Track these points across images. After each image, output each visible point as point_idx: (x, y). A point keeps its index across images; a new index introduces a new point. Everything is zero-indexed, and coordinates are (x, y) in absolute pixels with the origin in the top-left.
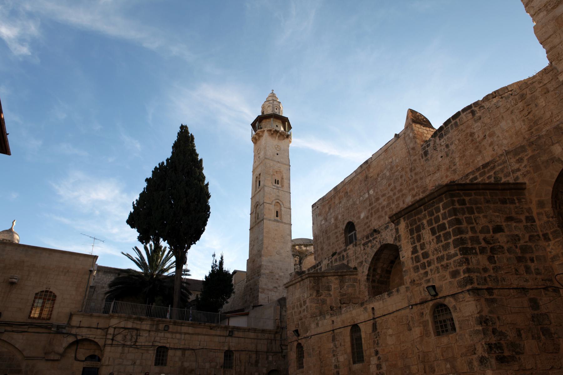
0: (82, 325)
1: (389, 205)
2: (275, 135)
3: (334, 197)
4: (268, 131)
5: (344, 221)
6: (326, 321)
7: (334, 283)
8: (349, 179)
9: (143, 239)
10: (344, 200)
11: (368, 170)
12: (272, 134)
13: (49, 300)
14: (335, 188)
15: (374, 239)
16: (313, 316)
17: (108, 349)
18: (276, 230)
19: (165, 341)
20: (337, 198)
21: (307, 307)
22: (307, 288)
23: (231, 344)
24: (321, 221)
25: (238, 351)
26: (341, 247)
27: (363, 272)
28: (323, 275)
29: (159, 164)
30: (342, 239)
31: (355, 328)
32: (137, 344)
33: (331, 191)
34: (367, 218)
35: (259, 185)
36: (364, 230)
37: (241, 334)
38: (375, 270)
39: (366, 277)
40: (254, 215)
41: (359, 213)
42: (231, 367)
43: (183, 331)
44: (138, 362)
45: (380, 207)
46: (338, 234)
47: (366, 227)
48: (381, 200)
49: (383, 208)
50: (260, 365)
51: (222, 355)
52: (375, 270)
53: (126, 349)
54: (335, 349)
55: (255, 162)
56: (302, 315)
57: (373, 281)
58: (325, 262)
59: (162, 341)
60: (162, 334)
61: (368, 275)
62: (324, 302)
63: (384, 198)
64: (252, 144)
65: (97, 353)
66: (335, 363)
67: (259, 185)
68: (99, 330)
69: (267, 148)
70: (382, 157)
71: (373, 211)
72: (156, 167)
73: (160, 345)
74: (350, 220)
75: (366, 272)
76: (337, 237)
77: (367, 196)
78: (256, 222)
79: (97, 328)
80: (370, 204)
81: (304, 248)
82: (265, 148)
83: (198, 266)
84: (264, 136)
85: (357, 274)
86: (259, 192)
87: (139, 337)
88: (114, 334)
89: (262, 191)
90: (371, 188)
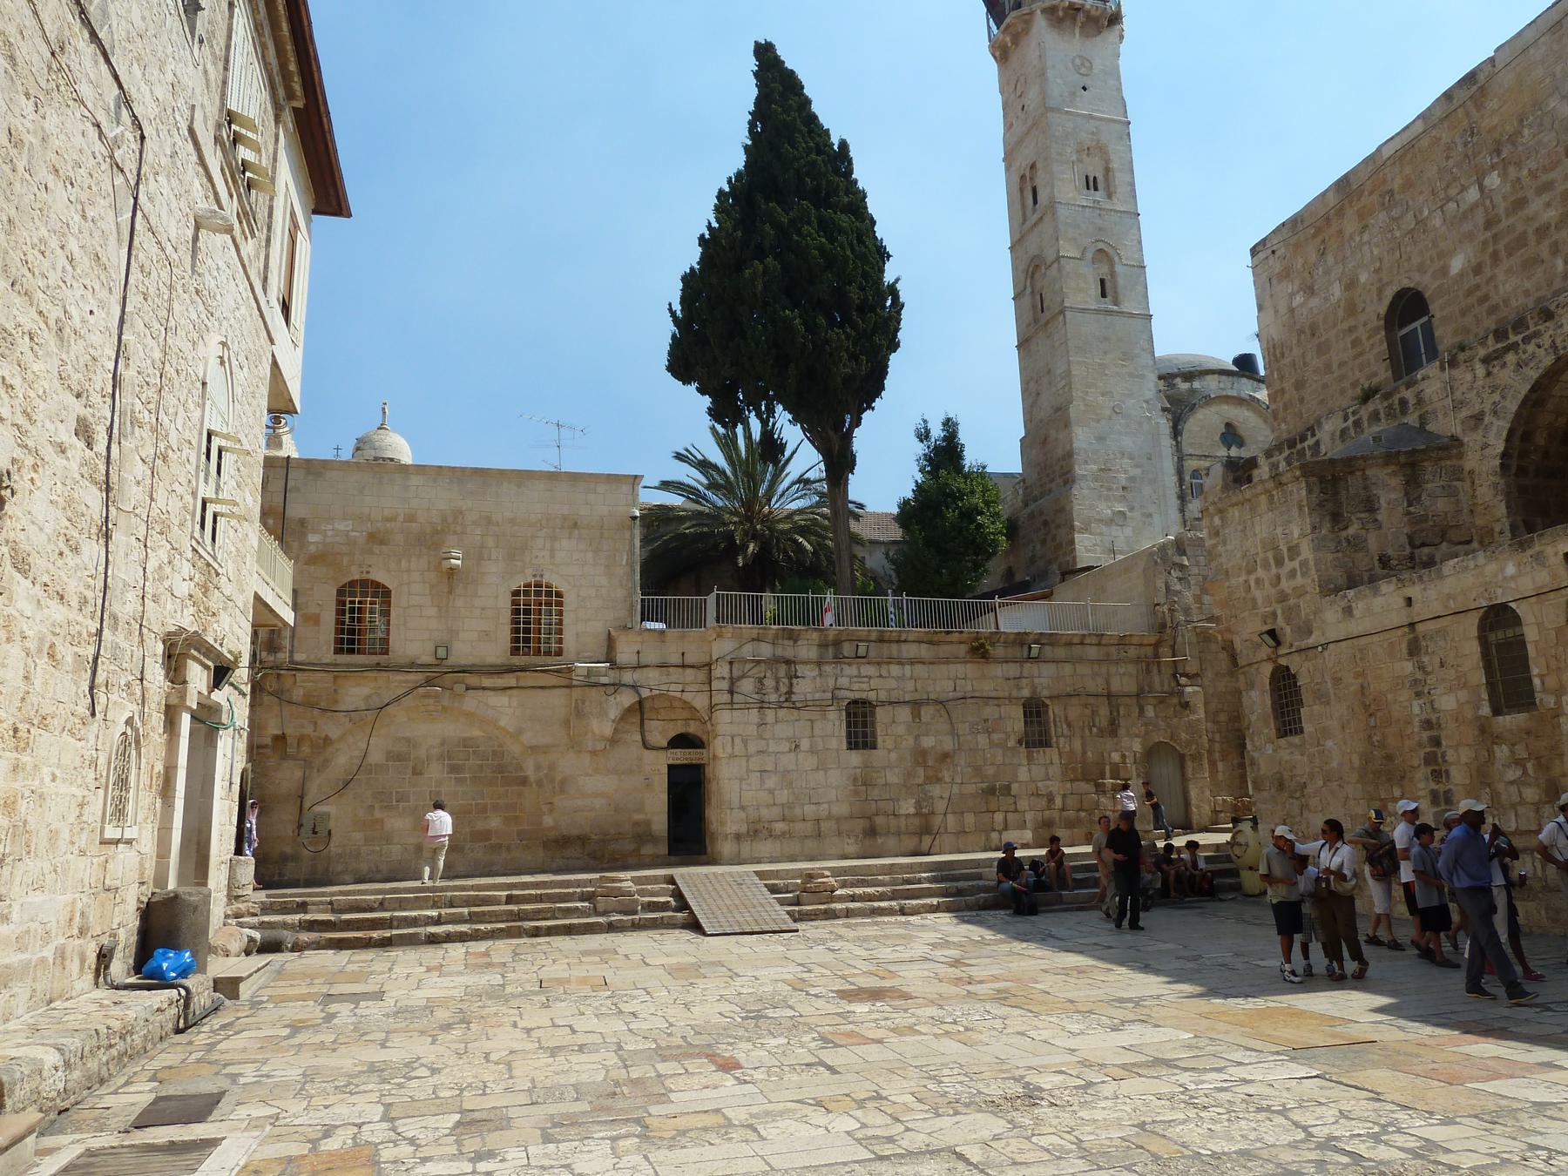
0: (644, 661)
2: (1068, 23)
3: (1340, 212)
4: (1044, 11)
5: (1380, 291)
6: (1378, 602)
7: (1388, 488)
8: (1397, 145)
9: (725, 413)
11: (1479, 106)
12: (1060, 21)
13: (549, 604)
14: (1343, 184)
15: (1526, 340)
16: (1329, 589)
17: (724, 718)
18: (1106, 339)
19: (865, 686)
20: (1350, 213)
21: (1304, 564)
22: (1301, 507)
23: (1036, 681)
24: (1292, 296)
25: (1058, 697)
26: (1376, 374)
27: (1485, 446)
28: (1349, 464)
29: (729, 181)
30: (1377, 347)
31: (1498, 618)
32: (794, 698)
33: (1324, 194)
34: (1478, 269)
35: (1035, 202)
36: (1463, 313)
37: (1061, 652)
38: (1527, 437)
39: (1498, 462)
40: (1027, 300)
42: (1045, 743)
43: (905, 655)
44: (805, 744)
45: (1530, 231)
46: (1362, 333)
47: (1473, 299)
48: (1536, 204)
49: (1542, 232)
50: (1122, 731)
51: (1018, 713)
52: (1527, 437)
53: (770, 715)
54: (1419, 675)
55: (1008, 127)
56: (1285, 584)
57: (1522, 471)
58: (1330, 427)
59: (856, 687)
60: (853, 670)
61: (1504, 455)
62: (1356, 544)
63: (1546, 197)
64: (991, 67)
65: (693, 729)
66: (1424, 716)
67: (1035, 202)
68: (689, 671)
69: (1050, 73)
70: (1536, 54)
71: (1501, 246)
72: (721, 192)
73: (852, 696)
74: (1407, 283)
75: (1500, 447)
76: (1356, 343)
77: (1473, 194)
78: (1036, 321)
79: (683, 666)
80: (1489, 224)
81: (1183, 386)
82: (1042, 74)
83: (885, 475)
84: (1034, 30)
85: (1460, 456)
86: (1035, 225)
87: (795, 681)
88: (731, 678)
89: (1047, 219)
90: (1493, 167)
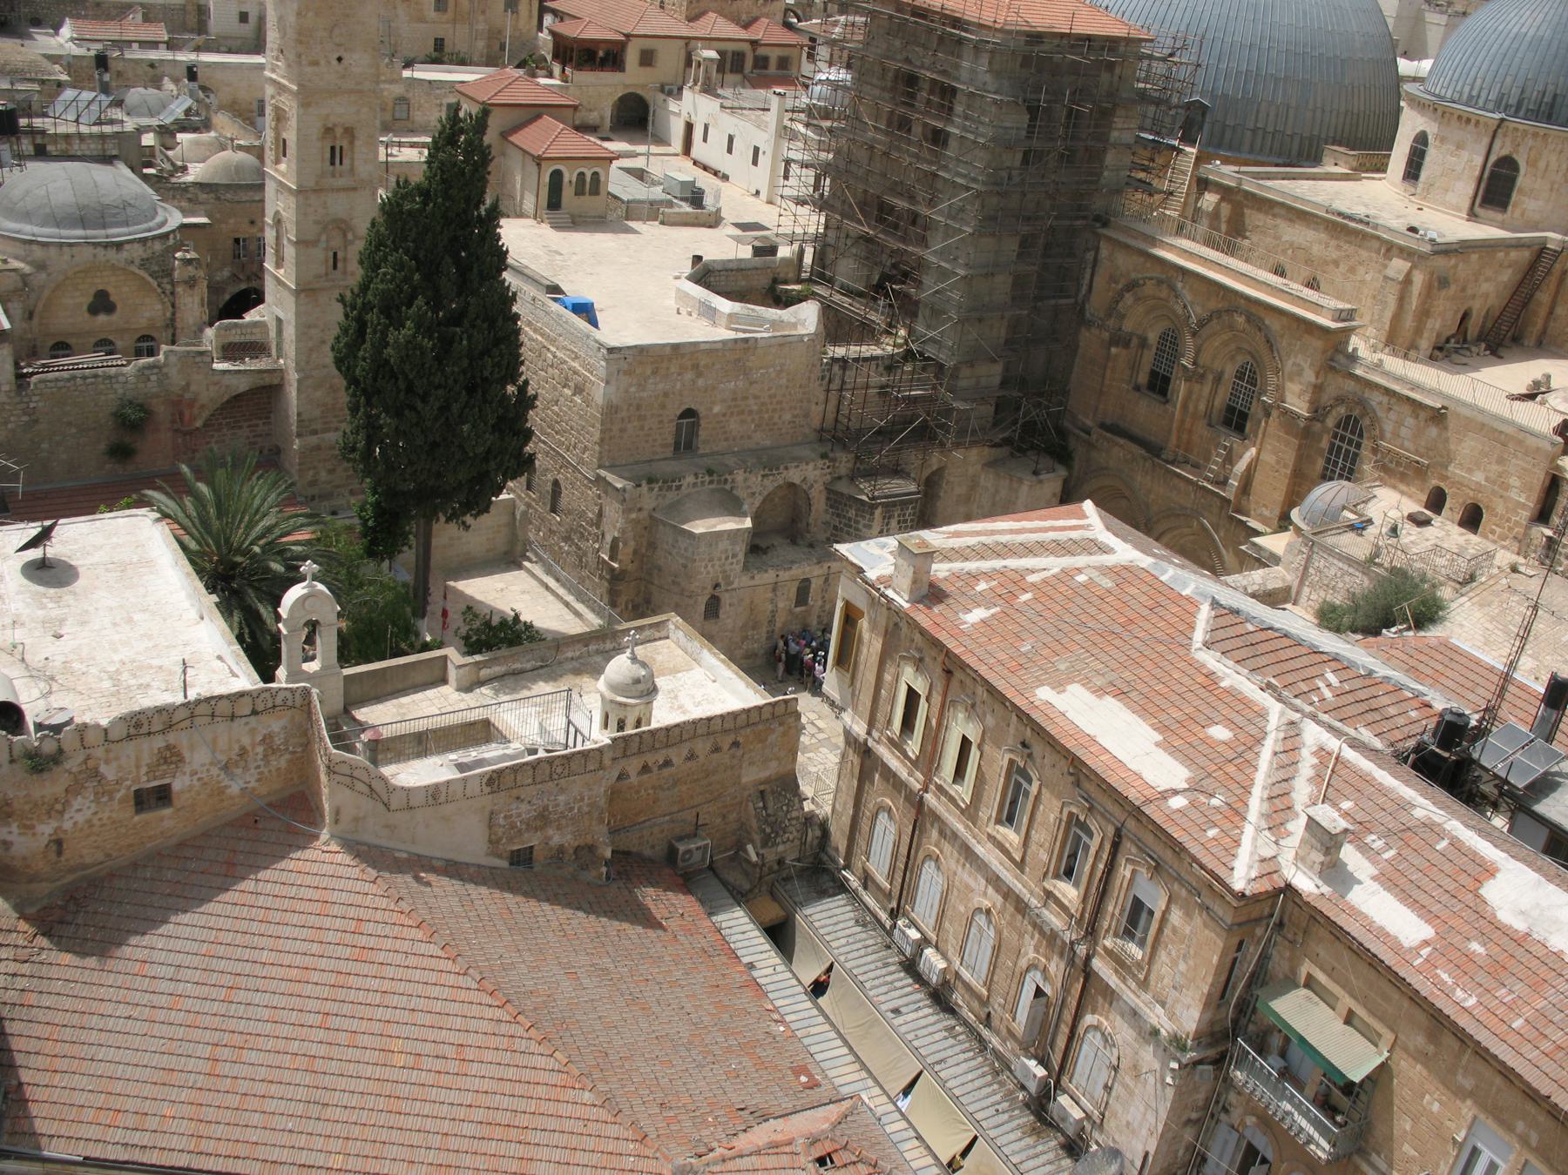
1: (760, 411)
3: (670, 360)
10: (689, 376)
14: (676, 347)
24: (630, 385)
40: (319, 254)
41: (713, 403)
48: (751, 401)
49: (751, 412)
76: (661, 422)
